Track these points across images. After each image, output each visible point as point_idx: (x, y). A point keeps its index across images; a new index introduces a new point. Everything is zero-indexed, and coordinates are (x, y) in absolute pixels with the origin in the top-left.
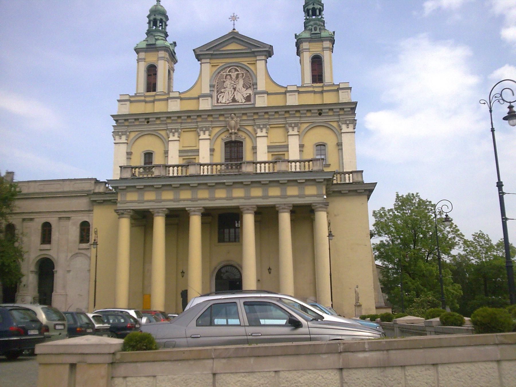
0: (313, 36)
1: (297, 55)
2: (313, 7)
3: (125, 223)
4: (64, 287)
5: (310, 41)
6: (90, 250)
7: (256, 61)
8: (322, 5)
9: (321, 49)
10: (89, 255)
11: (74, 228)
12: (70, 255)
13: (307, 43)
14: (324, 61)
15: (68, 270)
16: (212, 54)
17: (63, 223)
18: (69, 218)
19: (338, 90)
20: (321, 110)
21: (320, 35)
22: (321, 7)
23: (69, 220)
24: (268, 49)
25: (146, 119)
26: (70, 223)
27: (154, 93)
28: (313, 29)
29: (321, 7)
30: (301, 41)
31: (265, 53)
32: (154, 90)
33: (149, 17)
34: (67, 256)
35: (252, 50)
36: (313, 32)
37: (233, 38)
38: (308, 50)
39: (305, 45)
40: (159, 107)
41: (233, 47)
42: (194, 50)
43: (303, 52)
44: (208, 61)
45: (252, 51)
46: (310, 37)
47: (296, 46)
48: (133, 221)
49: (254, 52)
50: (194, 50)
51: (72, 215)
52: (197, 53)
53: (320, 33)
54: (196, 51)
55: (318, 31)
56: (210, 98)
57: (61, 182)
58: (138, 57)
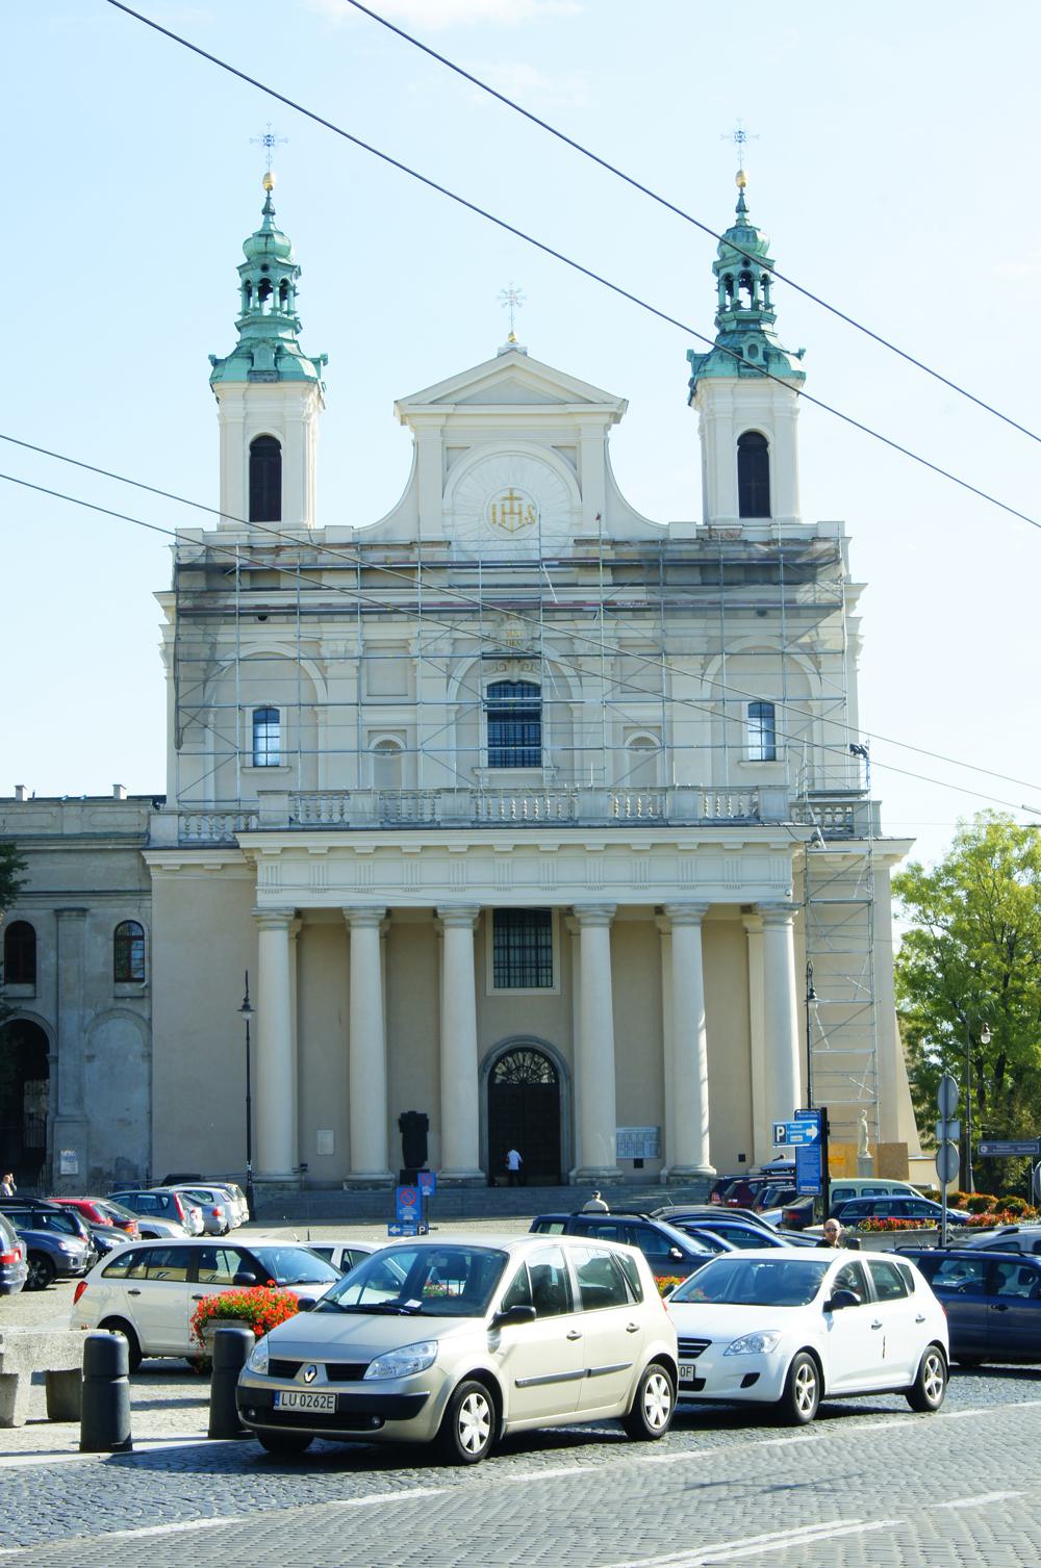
1: (689, 404)
2: (744, 269)
3: (275, 948)
4: (79, 1101)
6: (146, 1000)
10: (146, 1015)
11: (100, 939)
12: (90, 1013)
15: (87, 1053)
17: (69, 926)
18: (83, 911)
23: (85, 916)
26: (86, 924)
28: (745, 353)
33: (242, 269)
34: (83, 1017)
50: (396, 402)
51: (95, 904)
53: (767, 367)
57: (54, 809)
58: (221, 409)
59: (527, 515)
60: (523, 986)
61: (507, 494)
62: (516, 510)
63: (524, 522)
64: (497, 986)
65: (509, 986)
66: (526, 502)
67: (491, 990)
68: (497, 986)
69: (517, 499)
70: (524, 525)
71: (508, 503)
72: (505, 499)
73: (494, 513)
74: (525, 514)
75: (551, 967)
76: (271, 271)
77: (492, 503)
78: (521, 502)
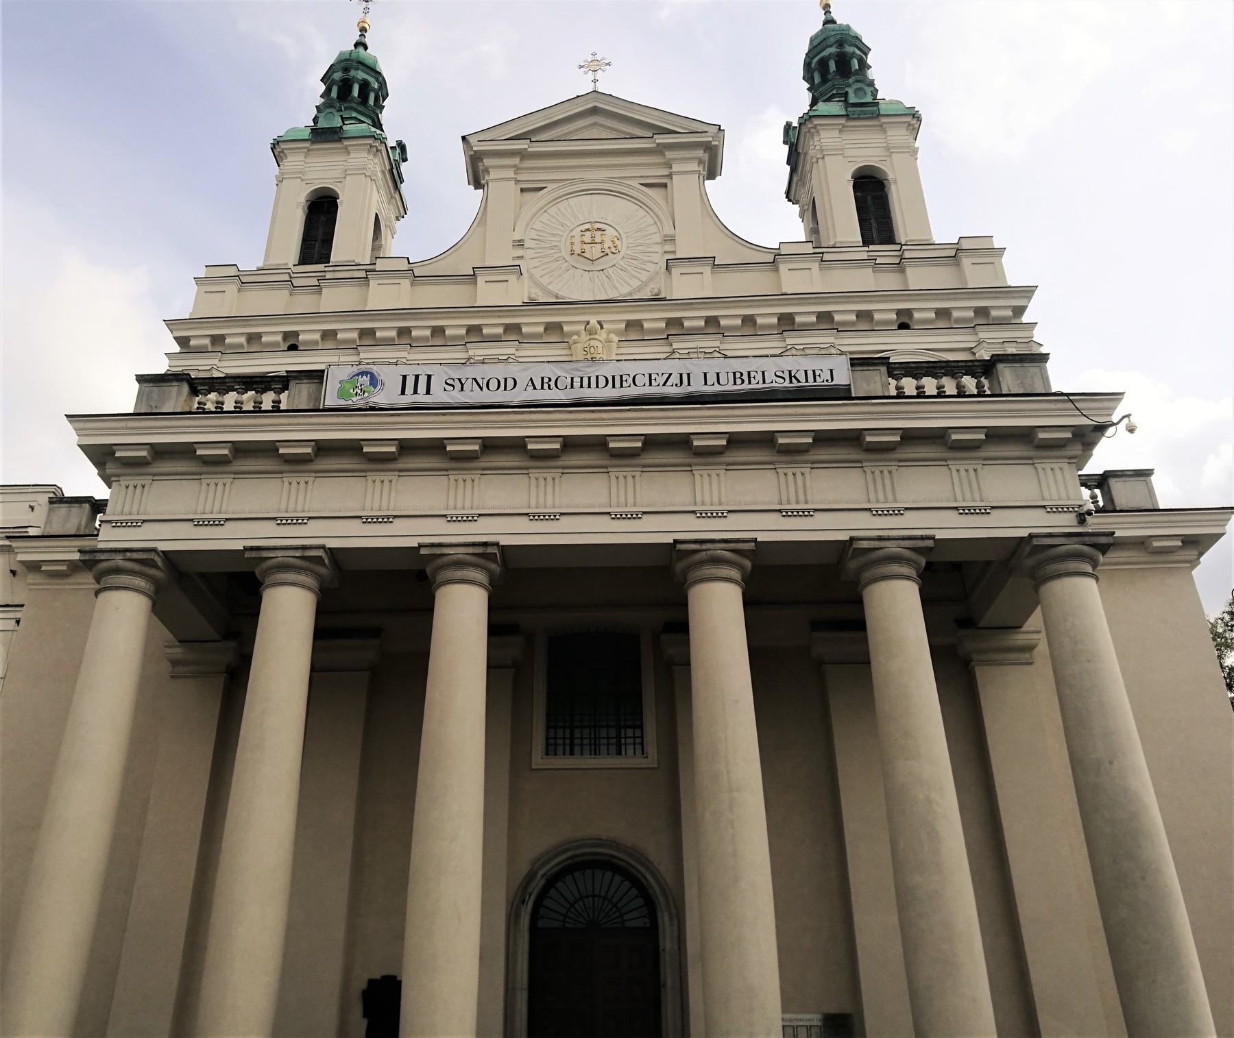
0: (854, 113)
5: (844, 126)
7: (670, 176)
8: (865, 50)
9: (881, 152)
13: (836, 133)
14: (895, 182)
16: (523, 155)
19: (956, 254)
20: (908, 313)
21: (875, 108)
22: (864, 57)
24: (711, 139)
25: (286, 335)
27: (321, 267)
29: (864, 57)
30: (815, 127)
31: (700, 153)
32: (325, 258)
35: (658, 141)
36: (852, 99)
37: (594, 111)
38: (840, 152)
39: (827, 138)
40: (336, 298)
41: (595, 136)
42: (464, 138)
43: (823, 158)
44: (510, 173)
45: (658, 144)
46: (844, 113)
47: (788, 163)
48: (178, 652)
49: (660, 150)
50: (464, 138)
52: (475, 149)
54: (472, 140)
55: (869, 99)
56: (512, 278)
59: (611, 244)
60: (595, 752)
61: (588, 226)
62: (598, 240)
63: (607, 251)
64: (551, 749)
65: (572, 753)
66: (610, 231)
67: (538, 759)
68: (551, 749)
69: (599, 229)
70: (607, 254)
71: (588, 234)
72: (588, 230)
73: (572, 243)
74: (608, 244)
75: (641, 727)
76: (353, 73)
77: (572, 234)
78: (603, 233)
